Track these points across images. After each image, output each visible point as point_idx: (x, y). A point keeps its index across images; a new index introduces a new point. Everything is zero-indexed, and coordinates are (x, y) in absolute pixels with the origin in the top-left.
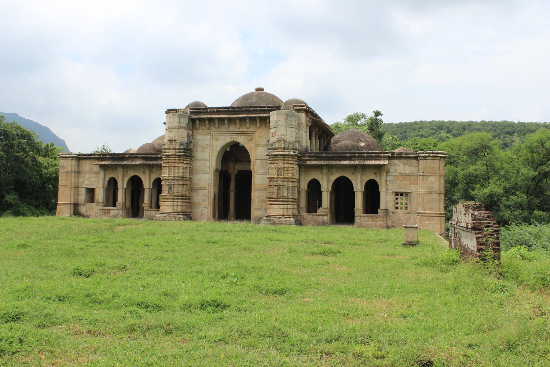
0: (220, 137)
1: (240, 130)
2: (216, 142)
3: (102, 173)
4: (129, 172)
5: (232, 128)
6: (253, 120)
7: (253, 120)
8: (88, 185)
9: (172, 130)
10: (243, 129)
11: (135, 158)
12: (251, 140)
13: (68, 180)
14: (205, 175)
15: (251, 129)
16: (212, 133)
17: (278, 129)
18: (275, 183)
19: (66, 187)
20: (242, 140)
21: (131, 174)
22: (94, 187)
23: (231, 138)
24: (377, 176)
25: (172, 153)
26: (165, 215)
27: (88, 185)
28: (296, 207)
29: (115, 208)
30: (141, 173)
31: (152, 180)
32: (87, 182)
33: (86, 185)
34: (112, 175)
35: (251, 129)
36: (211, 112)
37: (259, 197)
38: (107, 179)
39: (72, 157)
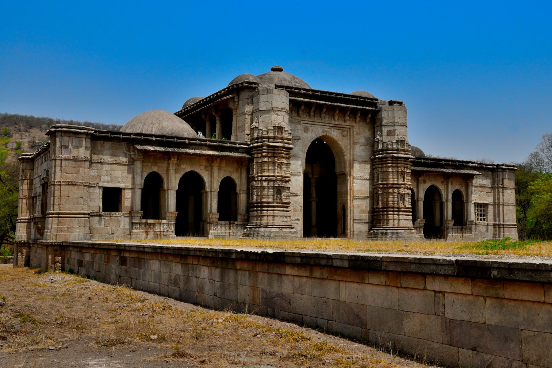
0: (311, 128)
1: (337, 123)
2: (305, 134)
3: (138, 165)
4: (183, 166)
5: (327, 119)
6: (354, 112)
7: (354, 112)
8: (108, 182)
9: (279, 113)
10: (341, 123)
11: (201, 145)
12: (345, 137)
13: (78, 172)
14: (297, 177)
15: (348, 123)
16: (302, 122)
17: (396, 128)
18: (396, 191)
19: (74, 184)
20: (335, 134)
21: (187, 168)
22: (122, 185)
23: (323, 131)
24: (462, 186)
25: (282, 145)
26: (277, 230)
27: (108, 182)
28: (411, 217)
29: (164, 221)
30: (203, 168)
31: (220, 180)
32: (106, 178)
33: (104, 182)
34: (155, 169)
35: (348, 123)
36: (304, 94)
37: (359, 206)
38: (145, 175)
39: (87, 134)
